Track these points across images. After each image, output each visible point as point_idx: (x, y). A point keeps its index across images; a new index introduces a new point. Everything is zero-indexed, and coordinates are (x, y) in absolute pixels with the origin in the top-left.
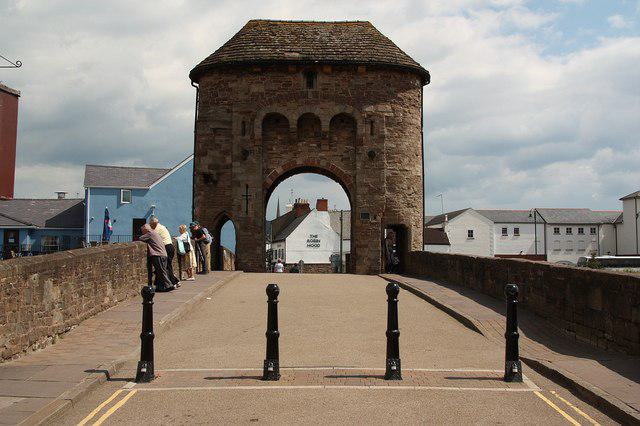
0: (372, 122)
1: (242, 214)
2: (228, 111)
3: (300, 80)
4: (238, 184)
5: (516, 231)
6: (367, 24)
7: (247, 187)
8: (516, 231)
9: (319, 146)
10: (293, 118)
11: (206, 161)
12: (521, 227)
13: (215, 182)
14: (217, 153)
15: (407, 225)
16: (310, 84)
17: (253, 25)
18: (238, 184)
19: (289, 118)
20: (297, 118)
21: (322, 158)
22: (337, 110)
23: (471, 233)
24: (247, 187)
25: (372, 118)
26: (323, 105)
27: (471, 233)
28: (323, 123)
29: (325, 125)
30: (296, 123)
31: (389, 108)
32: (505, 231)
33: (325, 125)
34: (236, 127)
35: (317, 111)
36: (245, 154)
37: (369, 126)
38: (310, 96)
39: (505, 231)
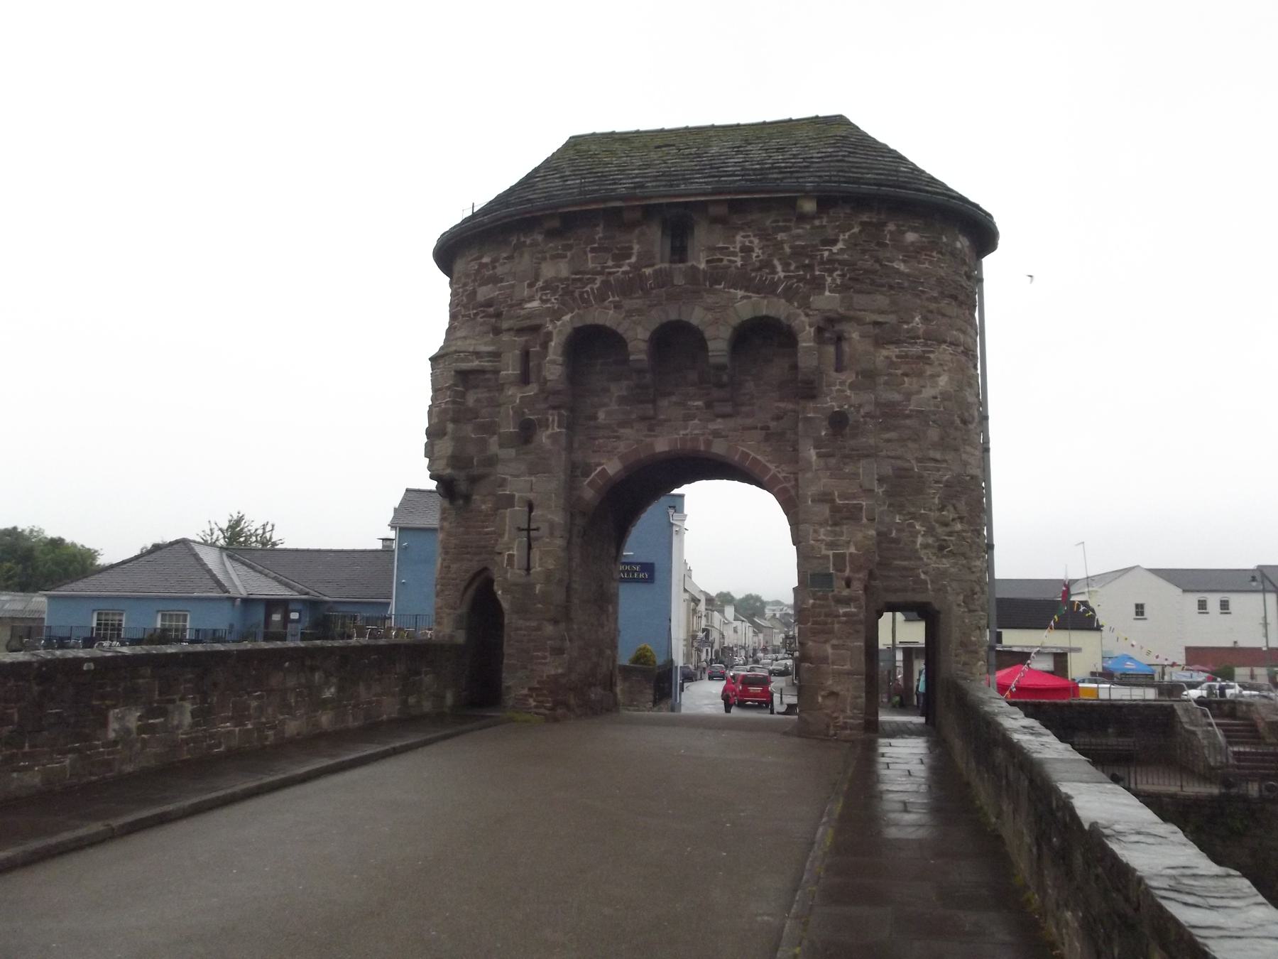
0: (839, 339)
1: (514, 574)
2: (497, 331)
3: (655, 236)
4: (509, 501)
5: (1224, 606)
6: (840, 121)
7: (531, 507)
8: (1224, 606)
9: (709, 405)
10: (638, 336)
11: (446, 447)
12: (1235, 600)
13: (467, 498)
14: (469, 430)
15: (937, 606)
16: (679, 253)
17: (575, 143)
18: (509, 501)
19: (628, 336)
20: (647, 335)
21: (716, 434)
22: (745, 306)
23: (1140, 609)
24: (531, 507)
25: (838, 327)
26: (710, 299)
27: (1140, 609)
28: (712, 345)
29: (718, 345)
30: (643, 346)
31: (881, 300)
32: (1202, 605)
33: (718, 345)
34: (510, 370)
35: (696, 316)
36: (527, 431)
37: (831, 349)
38: (679, 280)
39: (1202, 605)
